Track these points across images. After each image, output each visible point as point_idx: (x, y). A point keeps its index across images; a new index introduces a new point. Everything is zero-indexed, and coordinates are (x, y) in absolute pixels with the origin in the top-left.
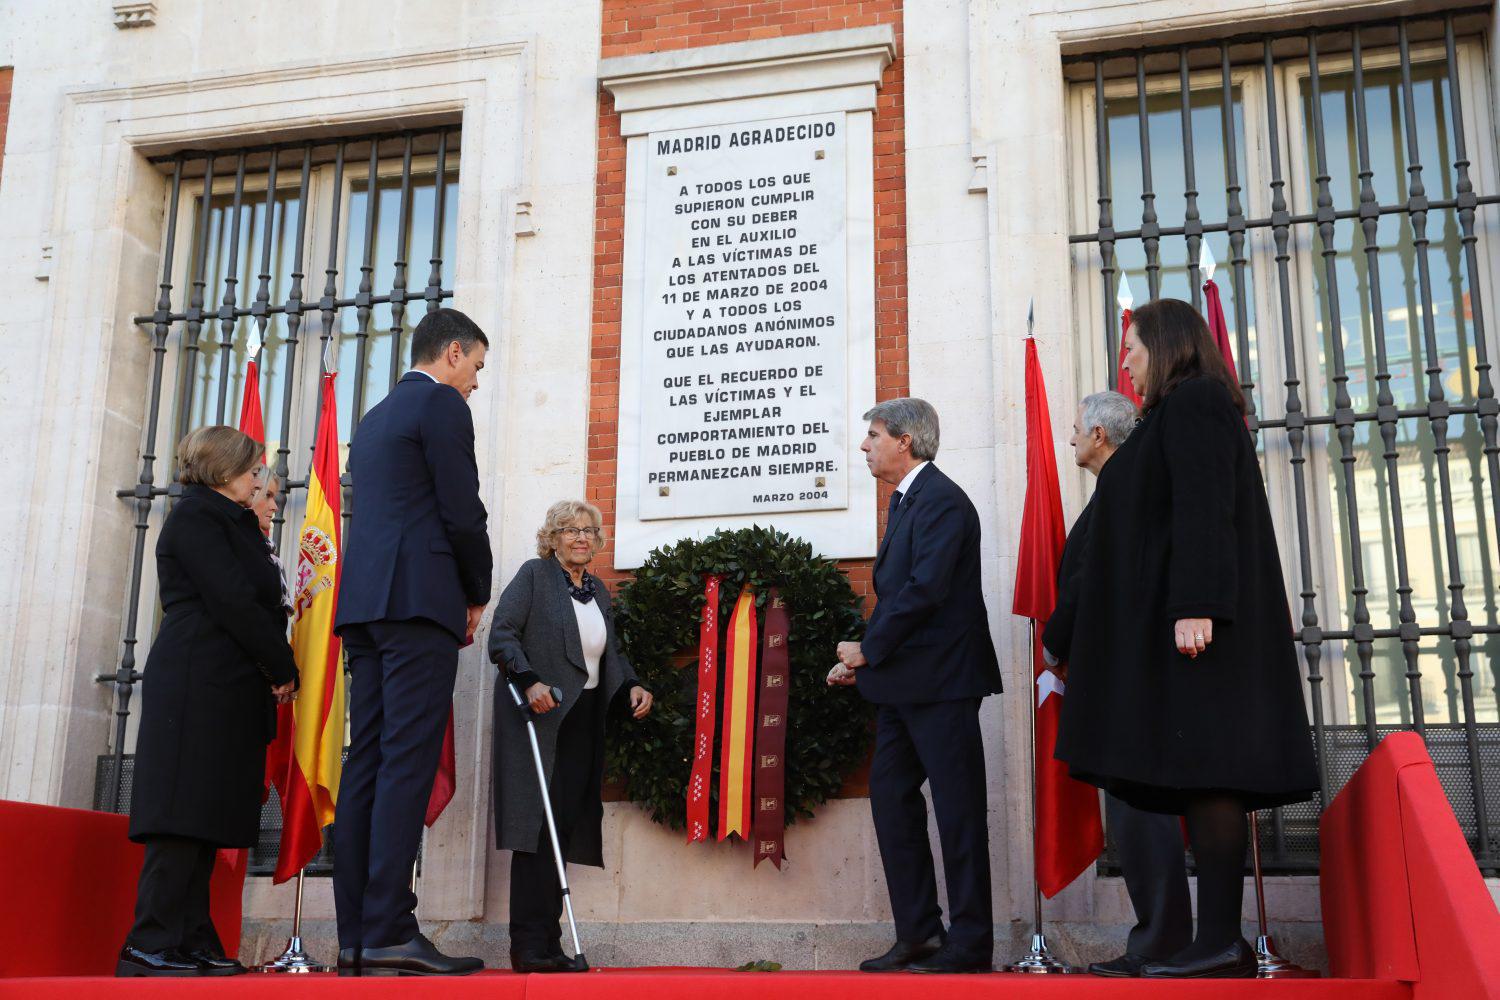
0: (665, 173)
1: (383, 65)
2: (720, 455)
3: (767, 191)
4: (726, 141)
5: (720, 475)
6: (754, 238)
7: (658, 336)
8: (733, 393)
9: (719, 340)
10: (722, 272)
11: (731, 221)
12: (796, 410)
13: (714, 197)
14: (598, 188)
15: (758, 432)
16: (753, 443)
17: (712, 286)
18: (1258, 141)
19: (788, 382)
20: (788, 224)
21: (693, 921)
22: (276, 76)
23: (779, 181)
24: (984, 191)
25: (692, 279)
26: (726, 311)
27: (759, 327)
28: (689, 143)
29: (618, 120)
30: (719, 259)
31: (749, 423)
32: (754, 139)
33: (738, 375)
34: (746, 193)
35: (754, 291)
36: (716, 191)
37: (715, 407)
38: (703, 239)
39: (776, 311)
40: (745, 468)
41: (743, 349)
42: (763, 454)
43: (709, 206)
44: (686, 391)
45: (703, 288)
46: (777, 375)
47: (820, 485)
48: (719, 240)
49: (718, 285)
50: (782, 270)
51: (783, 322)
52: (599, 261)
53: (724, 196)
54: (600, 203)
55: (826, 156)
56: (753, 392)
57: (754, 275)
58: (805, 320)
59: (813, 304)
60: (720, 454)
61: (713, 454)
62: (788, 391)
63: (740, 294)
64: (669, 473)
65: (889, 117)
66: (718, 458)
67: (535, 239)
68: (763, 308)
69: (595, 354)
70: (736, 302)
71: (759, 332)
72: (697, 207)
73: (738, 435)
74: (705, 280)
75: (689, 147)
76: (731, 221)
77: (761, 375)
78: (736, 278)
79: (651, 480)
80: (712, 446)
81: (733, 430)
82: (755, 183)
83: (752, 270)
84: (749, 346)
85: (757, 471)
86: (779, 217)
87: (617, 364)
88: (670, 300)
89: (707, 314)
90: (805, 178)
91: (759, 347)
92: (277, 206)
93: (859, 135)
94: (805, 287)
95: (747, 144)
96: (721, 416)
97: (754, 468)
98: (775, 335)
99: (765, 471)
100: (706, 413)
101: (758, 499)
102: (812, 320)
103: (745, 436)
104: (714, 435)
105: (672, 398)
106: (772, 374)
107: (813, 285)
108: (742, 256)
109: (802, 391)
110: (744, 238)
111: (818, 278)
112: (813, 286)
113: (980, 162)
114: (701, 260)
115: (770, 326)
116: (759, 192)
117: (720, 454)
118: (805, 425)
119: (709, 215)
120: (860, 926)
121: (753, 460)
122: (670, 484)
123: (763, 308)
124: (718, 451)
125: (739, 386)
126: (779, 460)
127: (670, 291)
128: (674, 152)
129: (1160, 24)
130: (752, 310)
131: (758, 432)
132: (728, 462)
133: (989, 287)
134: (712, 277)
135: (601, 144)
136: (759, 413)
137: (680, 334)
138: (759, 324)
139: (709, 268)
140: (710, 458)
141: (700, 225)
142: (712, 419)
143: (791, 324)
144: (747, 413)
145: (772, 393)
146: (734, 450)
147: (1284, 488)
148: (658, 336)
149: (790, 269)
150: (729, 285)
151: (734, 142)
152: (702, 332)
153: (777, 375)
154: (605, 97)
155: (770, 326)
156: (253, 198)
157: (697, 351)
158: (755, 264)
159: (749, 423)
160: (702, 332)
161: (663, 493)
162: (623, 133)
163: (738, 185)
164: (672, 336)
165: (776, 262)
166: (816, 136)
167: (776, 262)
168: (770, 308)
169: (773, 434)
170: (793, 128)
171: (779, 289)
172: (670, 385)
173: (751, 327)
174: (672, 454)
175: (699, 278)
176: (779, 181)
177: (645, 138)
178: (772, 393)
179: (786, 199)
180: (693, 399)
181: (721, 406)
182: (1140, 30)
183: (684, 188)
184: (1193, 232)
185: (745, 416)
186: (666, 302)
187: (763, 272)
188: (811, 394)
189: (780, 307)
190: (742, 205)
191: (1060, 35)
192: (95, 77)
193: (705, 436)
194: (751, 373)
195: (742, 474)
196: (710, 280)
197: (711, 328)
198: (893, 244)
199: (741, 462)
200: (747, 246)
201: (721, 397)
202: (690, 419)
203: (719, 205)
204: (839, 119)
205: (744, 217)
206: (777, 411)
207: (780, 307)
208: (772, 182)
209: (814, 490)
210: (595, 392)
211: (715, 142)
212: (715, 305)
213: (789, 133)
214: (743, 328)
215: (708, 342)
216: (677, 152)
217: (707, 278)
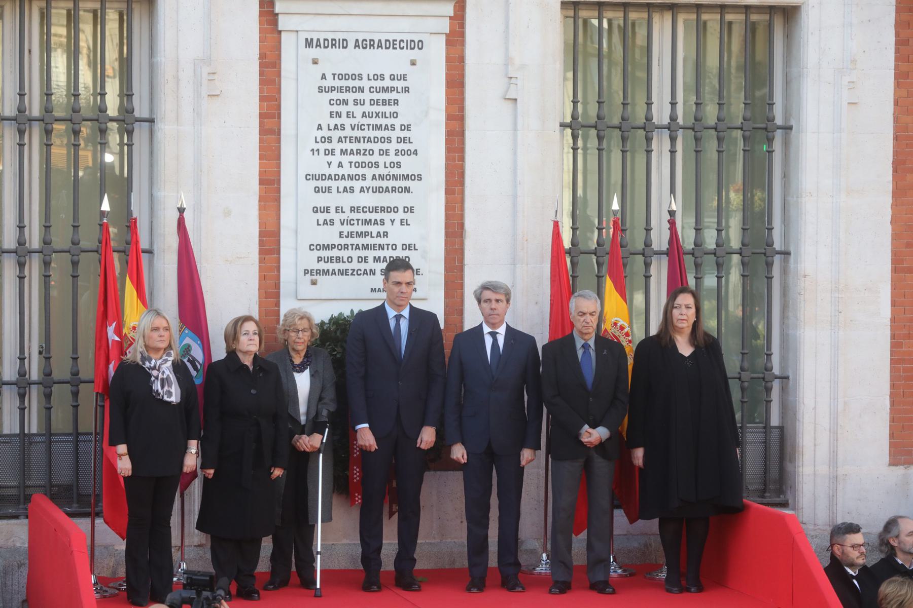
0: (311, 61)
4: (351, 44)
5: (350, 273)
6: (371, 115)
7: (308, 177)
8: (358, 220)
9: (348, 184)
10: (350, 137)
11: (356, 102)
12: (398, 235)
13: (344, 83)
14: (260, 63)
15: (373, 247)
16: (371, 254)
18: (659, 60)
19: (392, 215)
20: (393, 109)
21: (333, 543)
23: (387, 77)
24: (516, 100)
25: (330, 140)
26: (353, 164)
28: (326, 42)
30: (348, 127)
31: (368, 240)
32: (371, 45)
33: (361, 209)
34: (365, 84)
35: (371, 152)
36: (345, 79)
37: (346, 229)
38: (337, 112)
39: (385, 167)
41: (364, 192)
42: (377, 262)
43: (340, 90)
45: (338, 147)
46: (386, 210)
48: (348, 115)
49: (348, 146)
51: (390, 175)
52: (262, 116)
53: (351, 83)
54: (261, 74)
55: (418, 63)
56: (370, 220)
58: (403, 175)
59: (409, 165)
60: (350, 260)
61: (345, 260)
62: (393, 221)
63: (362, 153)
64: (317, 270)
66: (348, 262)
68: (377, 165)
69: (261, 182)
71: (374, 180)
73: (361, 248)
74: (339, 142)
76: (356, 102)
78: (359, 142)
79: (305, 274)
80: (344, 254)
81: (358, 245)
82: (371, 77)
84: (368, 189)
86: (387, 102)
87: (278, 190)
88: (316, 153)
89: (340, 165)
90: (404, 77)
91: (374, 190)
93: (437, 50)
95: (365, 48)
96: (350, 235)
97: (371, 270)
98: (384, 184)
100: (340, 232)
101: (373, 290)
102: (408, 175)
103: (365, 249)
104: (346, 247)
105: (318, 220)
106: (383, 209)
107: (409, 152)
108: (363, 127)
109: (401, 222)
110: (364, 115)
111: (412, 147)
112: (408, 153)
113: (513, 81)
114: (336, 126)
115: (382, 177)
116: (374, 83)
117: (350, 260)
118: (403, 245)
119: (341, 96)
120: (431, 543)
121: (371, 265)
122: (318, 277)
123: (377, 165)
124: (348, 258)
125: (362, 216)
127: (316, 146)
128: (316, 47)
130: (370, 165)
131: (373, 247)
132: (355, 265)
133: (515, 162)
134: (343, 139)
135: (261, 29)
136: (374, 234)
137: (322, 177)
138: (374, 175)
140: (343, 262)
141: (335, 102)
142: (344, 236)
143: (395, 177)
144: (367, 234)
145: (382, 222)
146: (359, 257)
147: (659, 283)
148: (308, 177)
149: (394, 140)
150: (355, 146)
151: (357, 46)
152: (337, 177)
153: (386, 210)
155: (382, 177)
157: (334, 190)
158: (372, 134)
159: (368, 240)
160: (337, 177)
161: (314, 283)
162: (280, 29)
163: (360, 77)
164: (317, 178)
165: (386, 134)
166: (411, 49)
167: (386, 134)
168: (381, 165)
169: (383, 249)
171: (387, 153)
172: (317, 212)
173: (369, 177)
174: (318, 257)
175: (335, 140)
176: (387, 77)
177: (295, 34)
178: (382, 222)
179: (391, 91)
180: (332, 222)
183: (324, 74)
185: (365, 236)
186: (313, 154)
187: (377, 140)
188: (407, 224)
189: (388, 165)
190: (363, 92)
193: (340, 247)
194: (369, 207)
195: (364, 274)
197: (343, 175)
198: (456, 124)
199: (363, 266)
200: (366, 121)
201: (350, 222)
202: (330, 235)
203: (348, 89)
205: (364, 100)
206: (386, 234)
207: (388, 165)
208: (382, 77)
210: (261, 208)
212: (346, 159)
213: (394, 44)
215: (342, 184)
216: (318, 47)
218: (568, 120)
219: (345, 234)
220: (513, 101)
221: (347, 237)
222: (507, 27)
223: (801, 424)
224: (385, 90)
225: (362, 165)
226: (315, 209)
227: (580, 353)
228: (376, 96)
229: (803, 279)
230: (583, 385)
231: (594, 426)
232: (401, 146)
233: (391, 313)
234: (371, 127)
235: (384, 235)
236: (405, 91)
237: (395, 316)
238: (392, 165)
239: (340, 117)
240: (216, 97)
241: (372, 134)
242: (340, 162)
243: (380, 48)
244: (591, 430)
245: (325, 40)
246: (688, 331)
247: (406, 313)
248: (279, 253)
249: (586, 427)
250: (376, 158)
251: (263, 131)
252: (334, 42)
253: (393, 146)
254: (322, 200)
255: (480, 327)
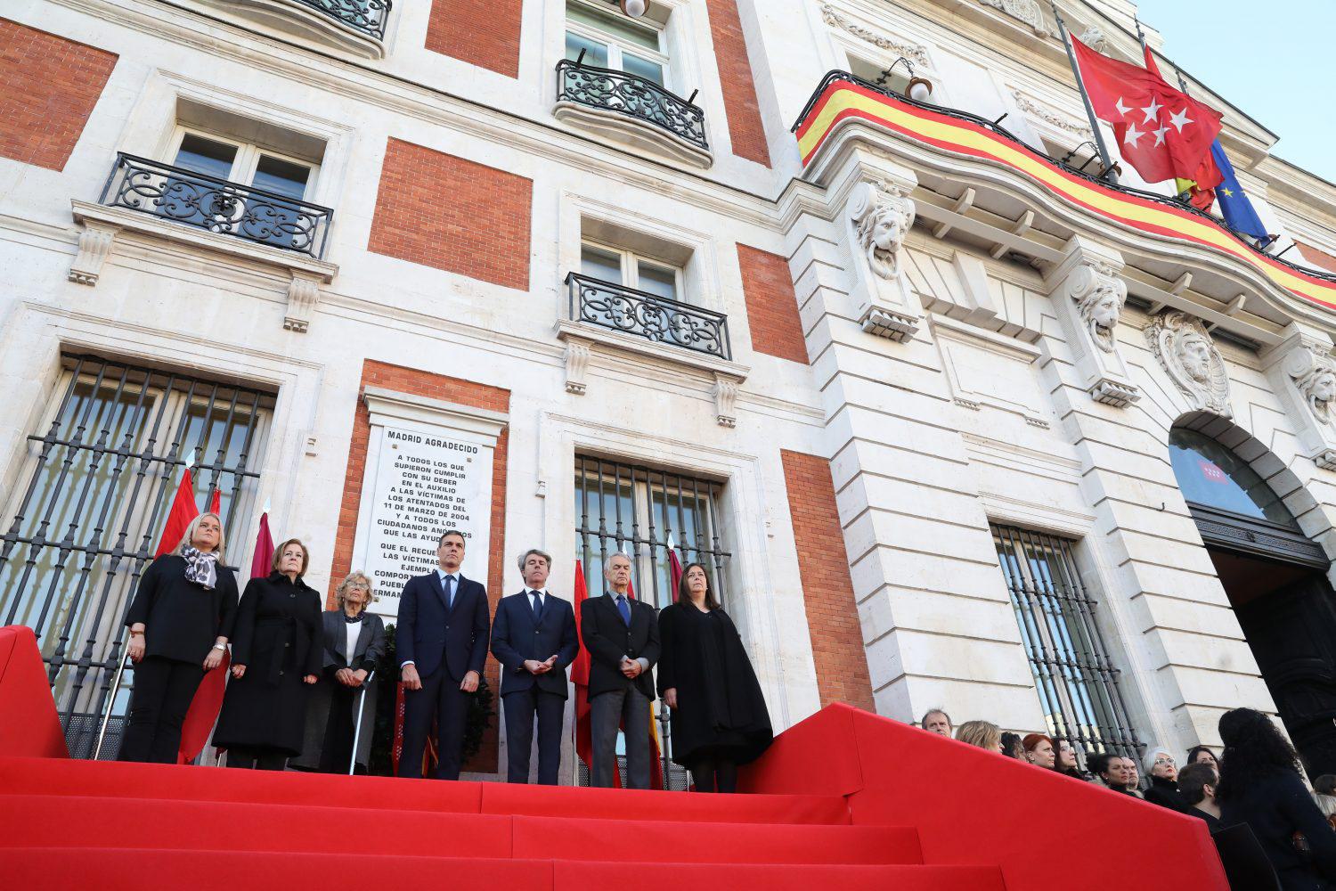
1: (240, 350)
3: (442, 469)
9: (412, 531)
11: (423, 478)
13: (415, 464)
17: (412, 505)
20: (452, 487)
22: (171, 335)
23: (449, 466)
24: (543, 497)
25: (401, 499)
27: (433, 530)
29: (369, 416)
34: (431, 467)
37: (408, 563)
43: (413, 468)
44: (391, 551)
45: (407, 505)
49: (415, 506)
50: (448, 507)
52: (348, 478)
53: (420, 465)
54: (351, 451)
56: (428, 560)
65: (501, 453)
67: (315, 458)
68: (436, 522)
70: (424, 516)
72: (406, 466)
84: (428, 538)
89: (407, 517)
92: (120, 407)
93: (486, 458)
96: (411, 568)
110: (429, 487)
112: (462, 518)
114: (406, 491)
123: (436, 522)
130: (431, 521)
137: (392, 524)
139: (411, 497)
149: (451, 507)
150: (420, 507)
152: (403, 526)
154: (362, 403)
156: (106, 395)
157: (400, 534)
158: (435, 500)
160: (403, 526)
163: (428, 462)
165: (446, 502)
167: (446, 502)
168: (440, 523)
171: (445, 515)
173: (430, 529)
175: (405, 499)
176: (449, 466)
177: (381, 428)
181: (411, 564)
182: (607, 451)
184: (619, 539)
187: (437, 505)
191: (575, 443)
192: (44, 299)
198: (497, 509)
201: (411, 559)
203: (418, 468)
204: (480, 448)
208: (445, 465)
210: (338, 542)
212: (412, 514)
215: (407, 531)
217: (408, 500)
221: (408, 569)
224: (448, 474)
225: (425, 520)
227: (616, 602)
228: (439, 476)
230: (622, 621)
231: (634, 657)
232: (457, 512)
233: (442, 574)
237: (446, 577)
240: (312, 458)
241: (435, 500)
244: (630, 661)
246: (703, 596)
247: (456, 576)
249: (626, 657)
250: (436, 517)
254: (389, 540)
255: (524, 591)
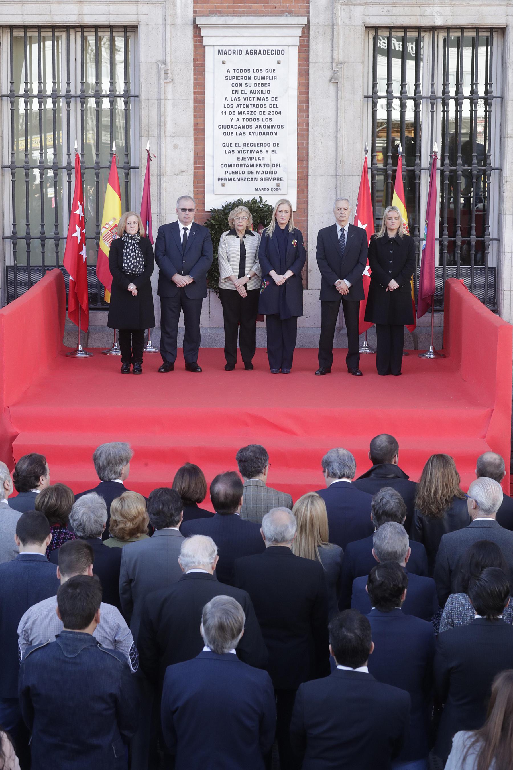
2: (243, 172)
3: (259, 74)
4: (244, 52)
7: (220, 127)
8: (248, 150)
9: (242, 130)
11: (246, 85)
12: (269, 158)
13: (240, 74)
15: (256, 165)
16: (255, 169)
19: (267, 148)
20: (267, 88)
23: (264, 71)
25: (232, 106)
26: (245, 120)
28: (230, 52)
31: (253, 162)
32: (255, 53)
34: (252, 75)
37: (241, 155)
38: (236, 91)
40: (252, 178)
41: (251, 135)
43: (238, 78)
45: (237, 110)
47: (278, 185)
49: (242, 109)
50: (265, 106)
53: (244, 74)
55: (281, 63)
57: (255, 107)
58: (273, 126)
59: (276, 120)
61: (241, 172)
62: (267, 151)
63: (250, 113)
68: (258, 120)
69: (195, 130)
70: (249, 116)
72: (233, 78)
73: (249, 166)
74: (237, 107)
75: (230, 53)
76: (246, 85)
77: (258, 145)
78: (248, 107)
79: (218, 180)
80: (240, 169)
81: (248, 164)
82: (255, 71)
83: (254, 105)
84: (253, 134)
85: (256, 179)
88: (224, 113)
89: (238, 120)
93: (293, 55)
94: (273, 113)
95: (252, 54)
96: (244, 159)
98: (262, 130)
99: (259, 179)
101: (256, 189)
104: (241, 165)
106: (262, 145)
110: (251, 92)
112: (276, 113)
115: (261, 127)
119: (238, 82)
121: (255, 175)
123: (258, 120)
125: (250, 148)
126: (264, 176)
127: (224, 110)
129: (399, 24)
130: (254, 120)
131: (256, 165)
132: (246, 175)
134: (240, 106)
135: (195, 46)
136: (257, 158)
137: (228, 127)
138: (257, 125)
139: (239, 103)
140: (239, 174)
141: (235, 85)
143: (269, 127)
144: (253, 158)
148: (220, 127)
149: (268, 106)
150: (246, 110)
151: (247, 53)
152: (236, 127)
154: (197, 29)
155: (261, 127)
157: (234, 134)
158: (256, 102)
159: (253, 162)
160: (236, 127)
161: (223, 185)
165: (263, 102)
166: (278, 54)
167: (263, 102)
168: (261, 120)
169: (262, 167)
170: (269, 50)
172: (225, 146)
173: (254, 127)
175: (235, 106)
176: (264, 71)
177: (213, 47)
180: (233, 152)
183: (228, 70)
187: (258, 106)
189: (264, 120)
190: (250, 79)
193: (238, 165)
195: (251, 180)
196: (239, 107)
197: (239, 126)
199: (250, 176)
200: (252, 95)
201: (243, 152)
202: (232, 159)
203: (242, 78)
206: (263, 158)
207: (264, 120)
208: (261, 71)
209: (276, 187)
210: (195, 144)
211: (240, 52)
212: (241, 117)
213: (268, 52)
214: (251, 127)
215: (239, 131)
217: (238, 106)
218: (370, 93)
219: (241, 158)
220: (335, 84)
222: (333, 42)
223: (503, 266)
224: (263, 78)
225: (250, 120)
226: (224, 145)
228: (257, 81)
229: (505, 184)
232: (272, 109)
234: (255, 99)
235: (262, 159)
236: (274, 78)
238: (267, 120)
239: (238, 93)
241: (256, 102)
242: (238, 119)
243: (260, 55)
245: (229, 50)
248: (205, 169)
250: (258, 116)
251: (195, 101)
252: (234, 52)
253: (267, 110)
254: (228, 139)
